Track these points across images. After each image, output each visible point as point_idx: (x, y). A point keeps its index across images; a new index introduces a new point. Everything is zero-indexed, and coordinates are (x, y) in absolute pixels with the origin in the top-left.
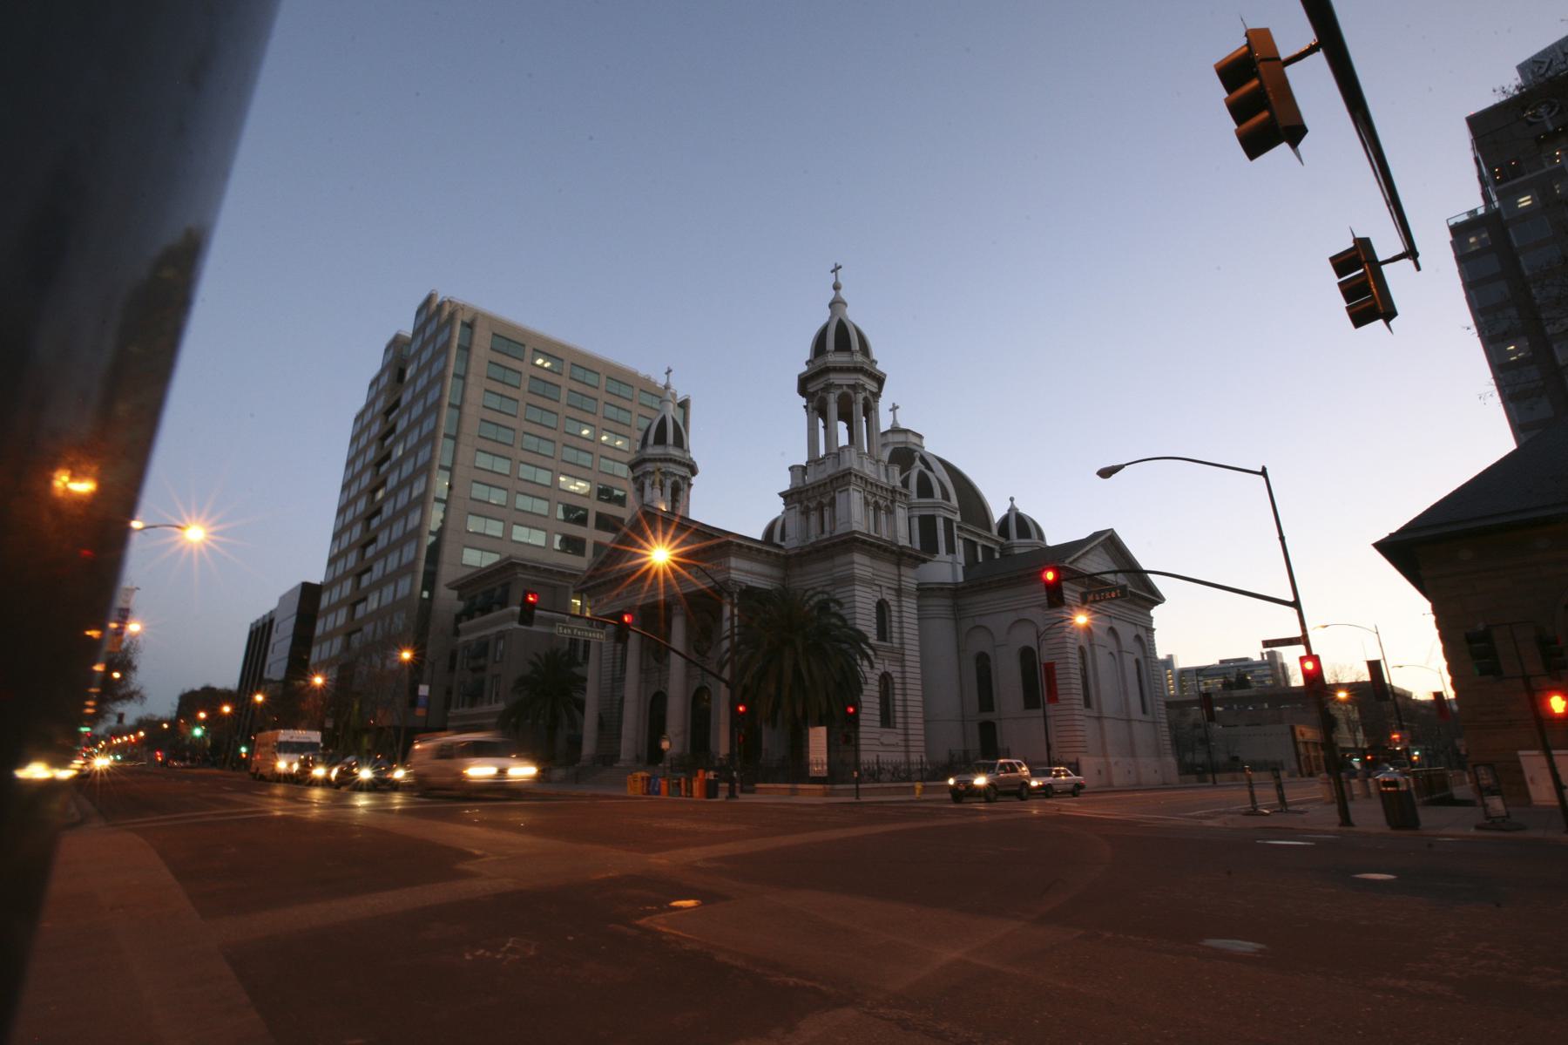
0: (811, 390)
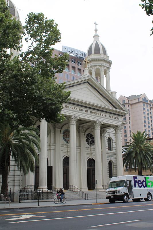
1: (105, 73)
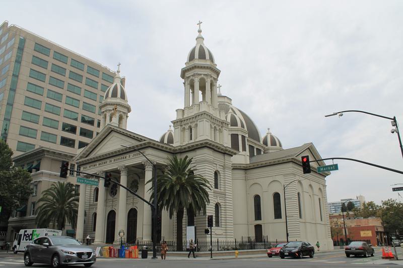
0: (188, 76)
1: (212, 85)
